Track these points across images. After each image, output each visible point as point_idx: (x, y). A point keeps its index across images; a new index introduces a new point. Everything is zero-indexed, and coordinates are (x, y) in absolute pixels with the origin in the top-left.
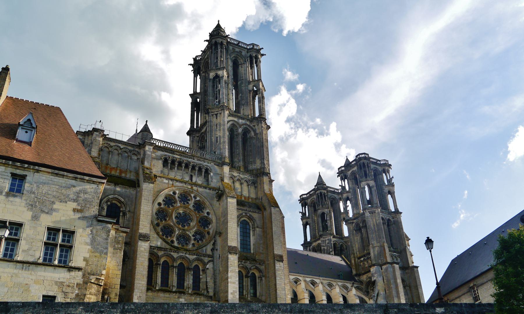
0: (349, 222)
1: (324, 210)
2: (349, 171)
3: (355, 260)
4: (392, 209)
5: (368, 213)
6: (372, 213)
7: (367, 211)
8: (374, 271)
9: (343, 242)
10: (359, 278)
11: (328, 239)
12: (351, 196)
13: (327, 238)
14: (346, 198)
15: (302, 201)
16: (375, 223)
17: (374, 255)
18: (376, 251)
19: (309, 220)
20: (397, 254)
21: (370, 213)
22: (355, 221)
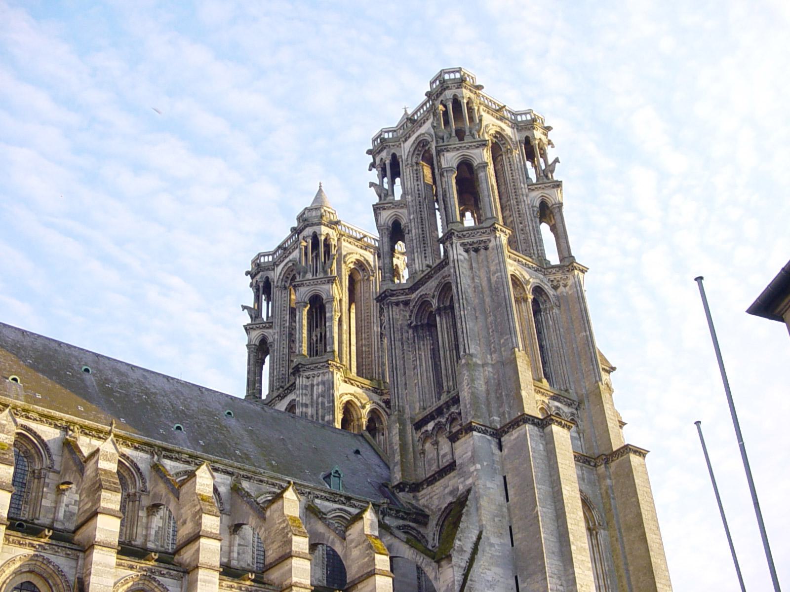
0: (394, 299)
1: (319, 287)
2: (406, 140)
3: (402, 433)
4: (553, 258)
5: (461, 250)
6: (476, 250)
7: (454, 240)
8: (469, 454)
9: (379, 402)
10: (415, 497)
11: (323, 383)
12: (409, 214)
13: (320, 379)
14: (390, 224)
15: (256, 274)
16: (485, 283)
17: (472, 393)
18: (482, 382)
19: (270, 331)
20: (566, 409)
21: (467, 251)
22: (414, 296)
